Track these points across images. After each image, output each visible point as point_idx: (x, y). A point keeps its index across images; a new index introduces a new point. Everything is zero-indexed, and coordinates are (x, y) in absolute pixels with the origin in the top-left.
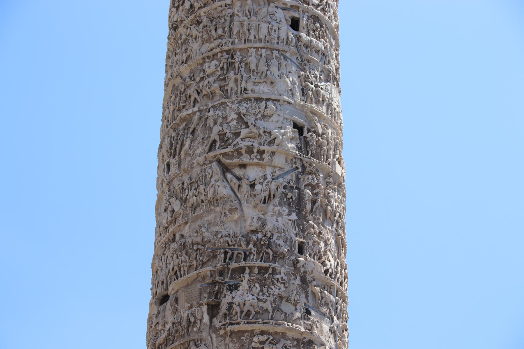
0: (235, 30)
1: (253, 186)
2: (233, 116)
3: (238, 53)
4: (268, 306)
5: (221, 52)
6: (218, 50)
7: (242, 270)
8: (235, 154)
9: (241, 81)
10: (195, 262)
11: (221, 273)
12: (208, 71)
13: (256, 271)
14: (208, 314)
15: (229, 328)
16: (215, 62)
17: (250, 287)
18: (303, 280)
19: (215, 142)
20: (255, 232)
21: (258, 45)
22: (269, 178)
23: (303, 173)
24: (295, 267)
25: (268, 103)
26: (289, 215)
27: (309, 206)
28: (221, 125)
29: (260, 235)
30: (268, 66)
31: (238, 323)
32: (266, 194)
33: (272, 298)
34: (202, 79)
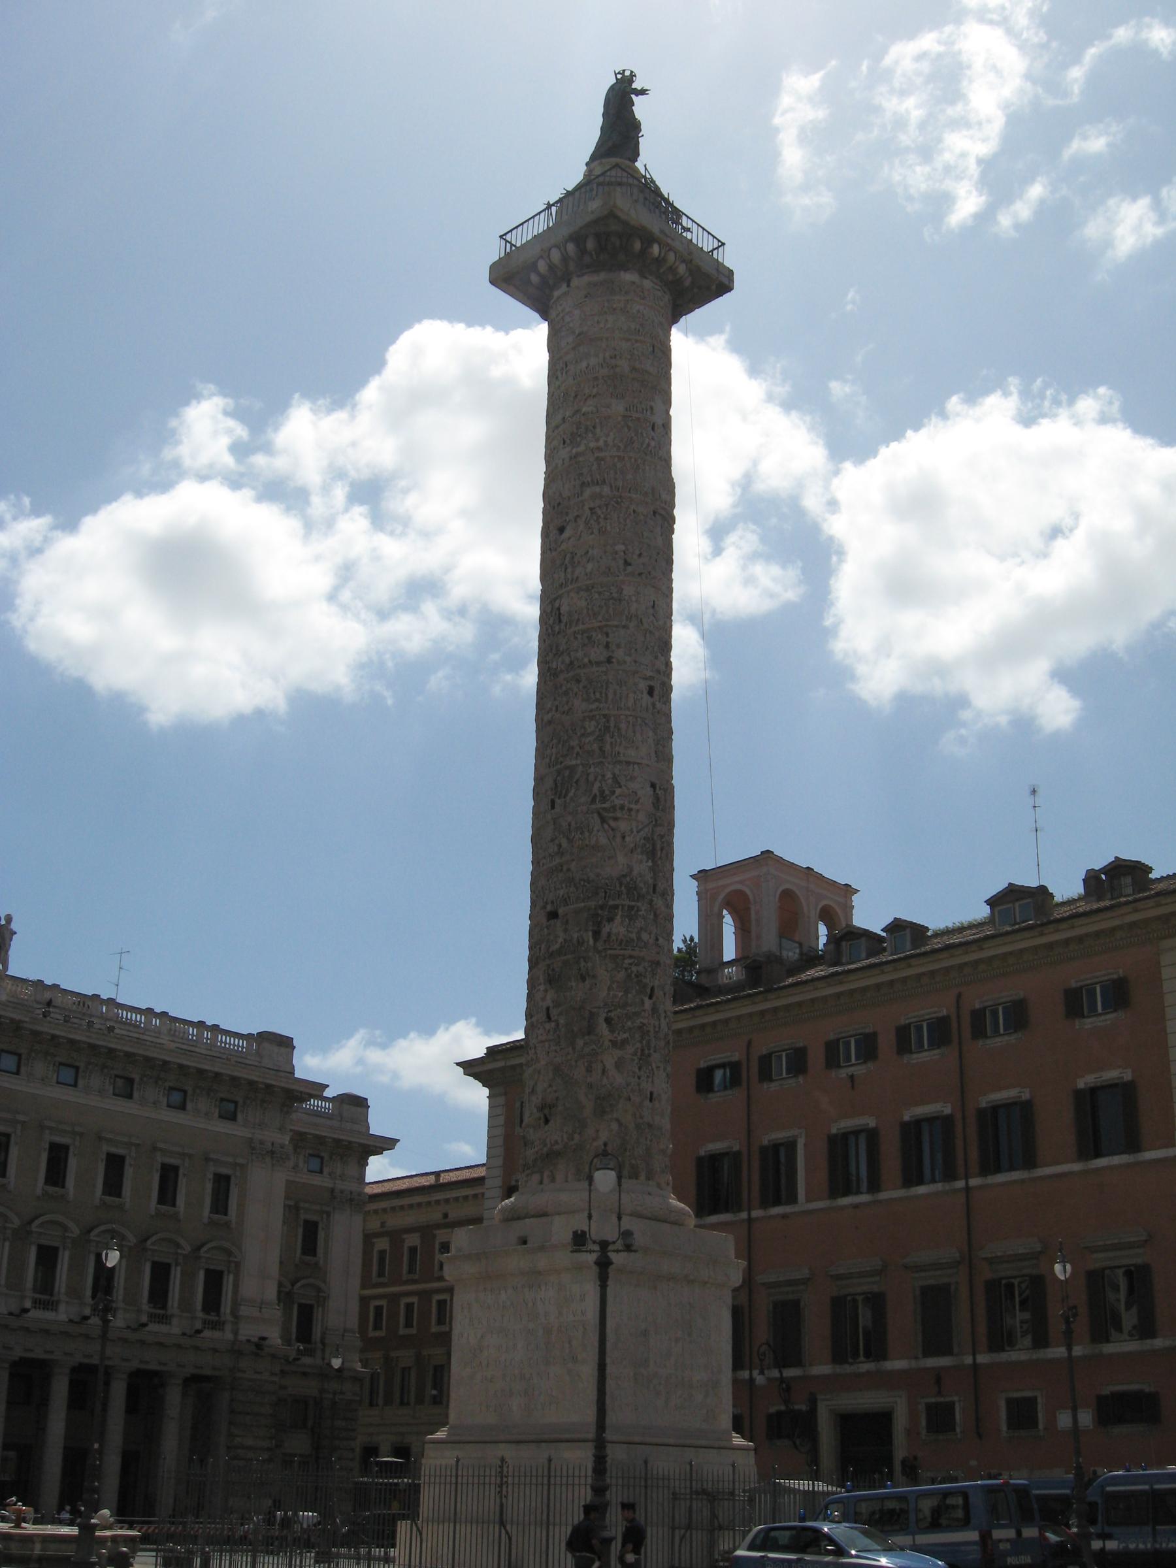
0: (610, 696)
1: (624, 837)
2: (609, 775)
3: (612, 718)
4: (634, 936)
5: (599, 715)
6: (596, 713)
7: (616, 907)
8: (611, 810)
9: (616, 745)
10: (582, 895)
11: (602, 907)
12: (589, 731)
13: (626, 908)
14: (593, 937)
15: (609, 952)
16: (593, 723)
17: (622, 920)
18: (656, 915)
19: (595, 795)
20: (624, 876)
21: (628, 713)
22: (635, 830)
23: (655, 826)
24: (650, 904)
25: (635, 766)
26: (647, 862)
27: (659, 853)
28: (600, 782)
29: (628, 879)
30: (634, 732)
31: (615, 949)
32: (632, 845)
33: (636, 930)
34: (583, 735)
